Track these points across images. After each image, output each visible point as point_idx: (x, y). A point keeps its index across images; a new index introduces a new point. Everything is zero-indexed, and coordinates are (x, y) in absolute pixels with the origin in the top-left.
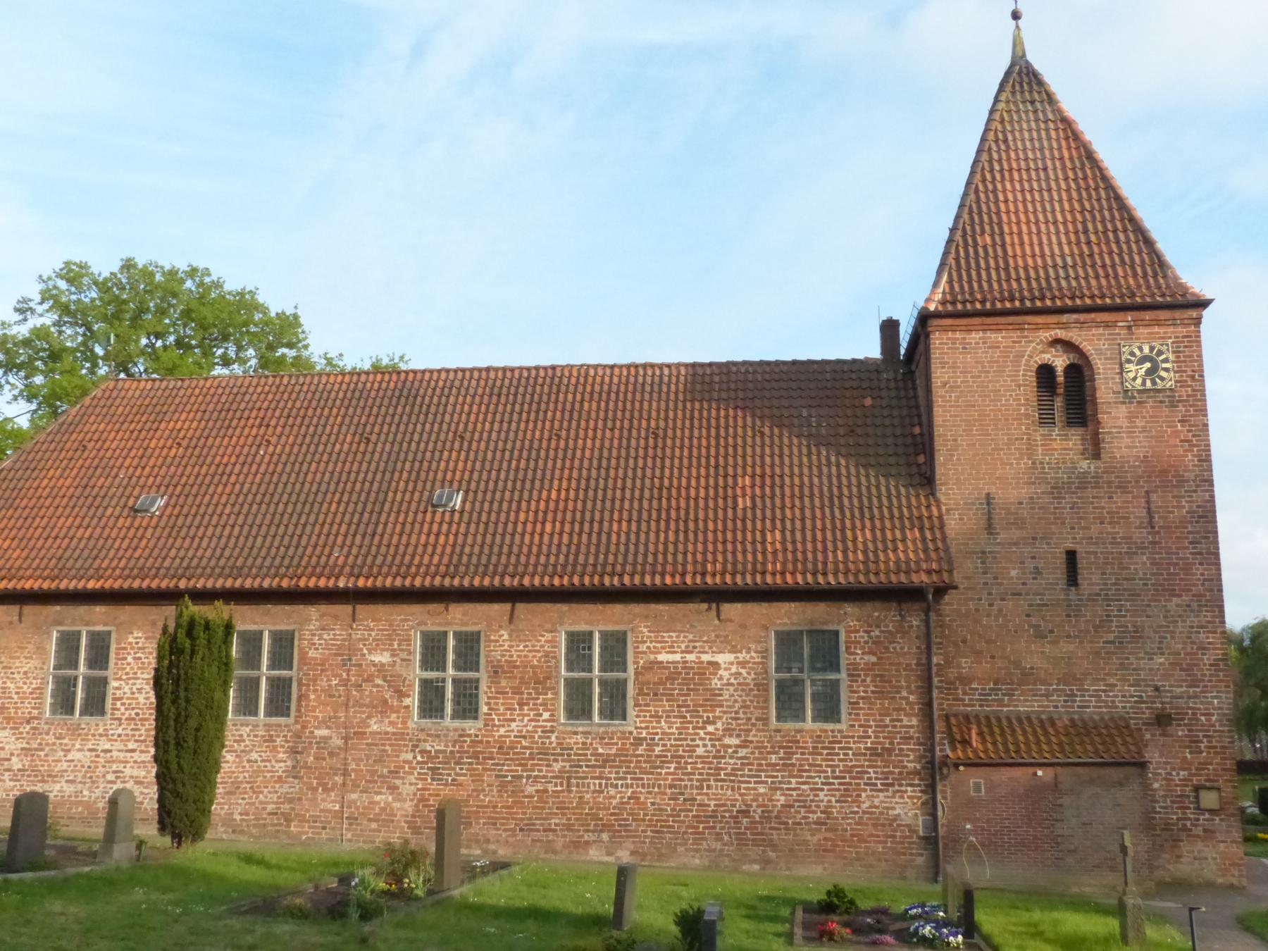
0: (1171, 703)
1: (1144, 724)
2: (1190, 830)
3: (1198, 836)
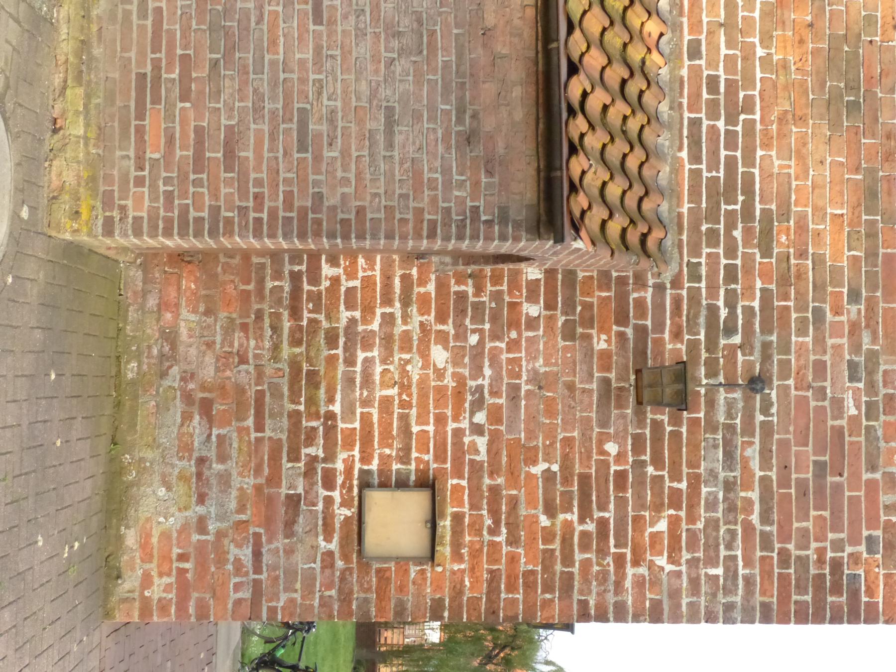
0: (712, 427)
1: (641, 331)
2: (294, 457)
3: (274, 479)
